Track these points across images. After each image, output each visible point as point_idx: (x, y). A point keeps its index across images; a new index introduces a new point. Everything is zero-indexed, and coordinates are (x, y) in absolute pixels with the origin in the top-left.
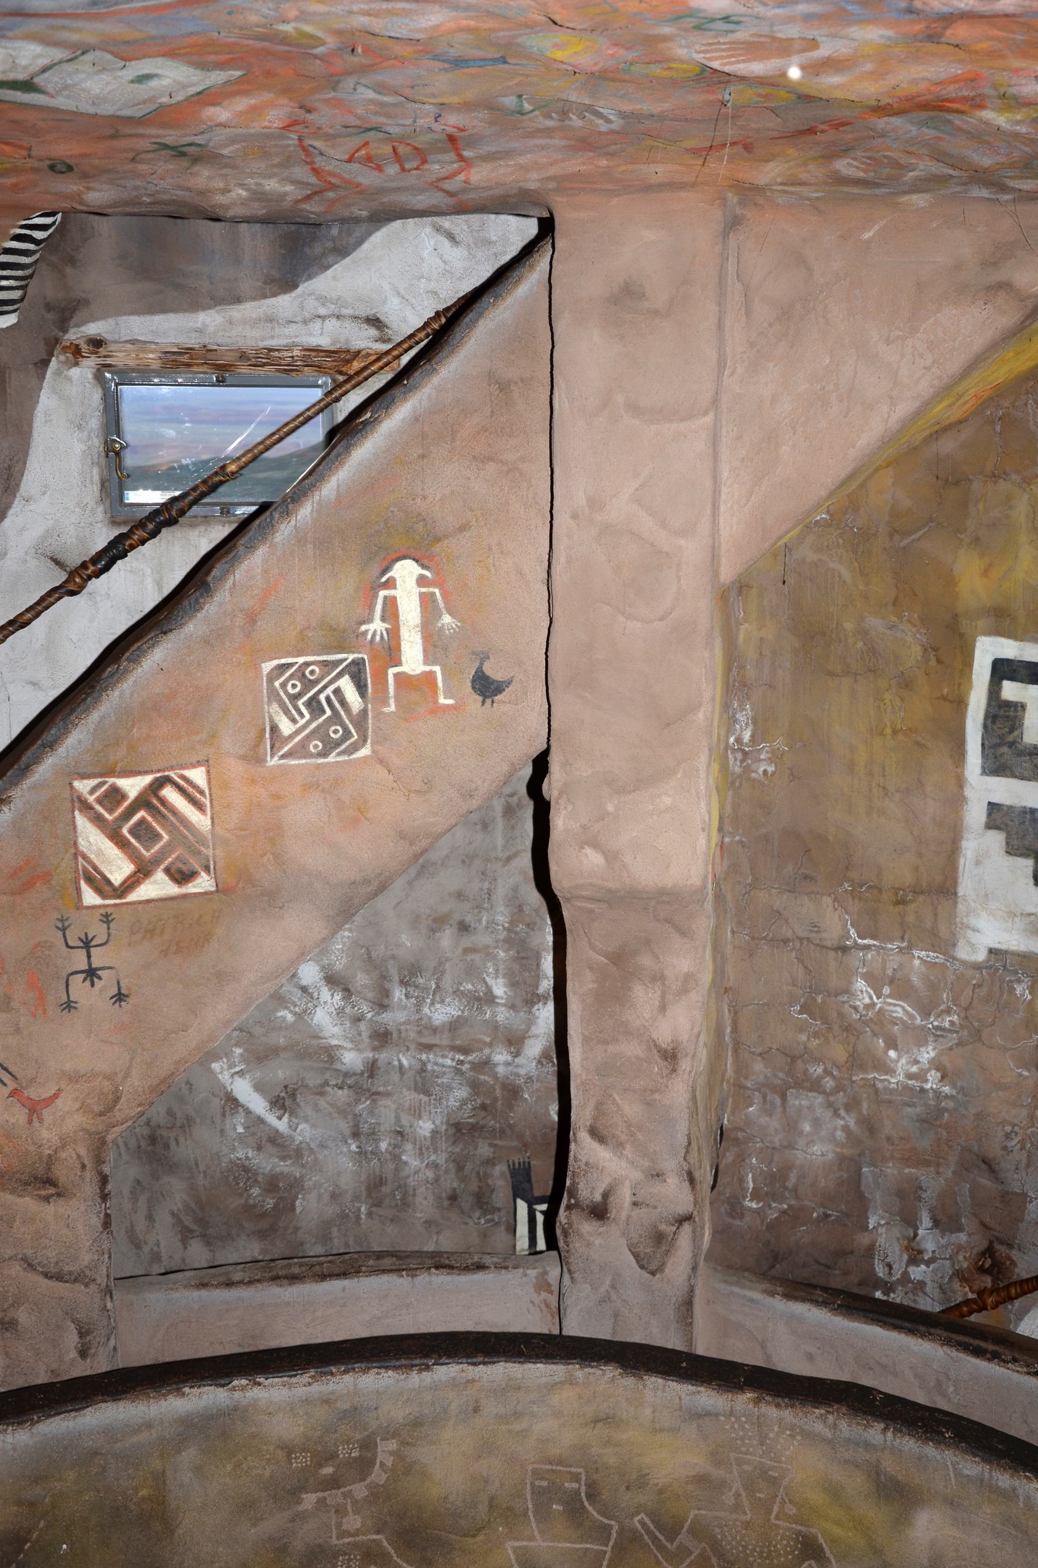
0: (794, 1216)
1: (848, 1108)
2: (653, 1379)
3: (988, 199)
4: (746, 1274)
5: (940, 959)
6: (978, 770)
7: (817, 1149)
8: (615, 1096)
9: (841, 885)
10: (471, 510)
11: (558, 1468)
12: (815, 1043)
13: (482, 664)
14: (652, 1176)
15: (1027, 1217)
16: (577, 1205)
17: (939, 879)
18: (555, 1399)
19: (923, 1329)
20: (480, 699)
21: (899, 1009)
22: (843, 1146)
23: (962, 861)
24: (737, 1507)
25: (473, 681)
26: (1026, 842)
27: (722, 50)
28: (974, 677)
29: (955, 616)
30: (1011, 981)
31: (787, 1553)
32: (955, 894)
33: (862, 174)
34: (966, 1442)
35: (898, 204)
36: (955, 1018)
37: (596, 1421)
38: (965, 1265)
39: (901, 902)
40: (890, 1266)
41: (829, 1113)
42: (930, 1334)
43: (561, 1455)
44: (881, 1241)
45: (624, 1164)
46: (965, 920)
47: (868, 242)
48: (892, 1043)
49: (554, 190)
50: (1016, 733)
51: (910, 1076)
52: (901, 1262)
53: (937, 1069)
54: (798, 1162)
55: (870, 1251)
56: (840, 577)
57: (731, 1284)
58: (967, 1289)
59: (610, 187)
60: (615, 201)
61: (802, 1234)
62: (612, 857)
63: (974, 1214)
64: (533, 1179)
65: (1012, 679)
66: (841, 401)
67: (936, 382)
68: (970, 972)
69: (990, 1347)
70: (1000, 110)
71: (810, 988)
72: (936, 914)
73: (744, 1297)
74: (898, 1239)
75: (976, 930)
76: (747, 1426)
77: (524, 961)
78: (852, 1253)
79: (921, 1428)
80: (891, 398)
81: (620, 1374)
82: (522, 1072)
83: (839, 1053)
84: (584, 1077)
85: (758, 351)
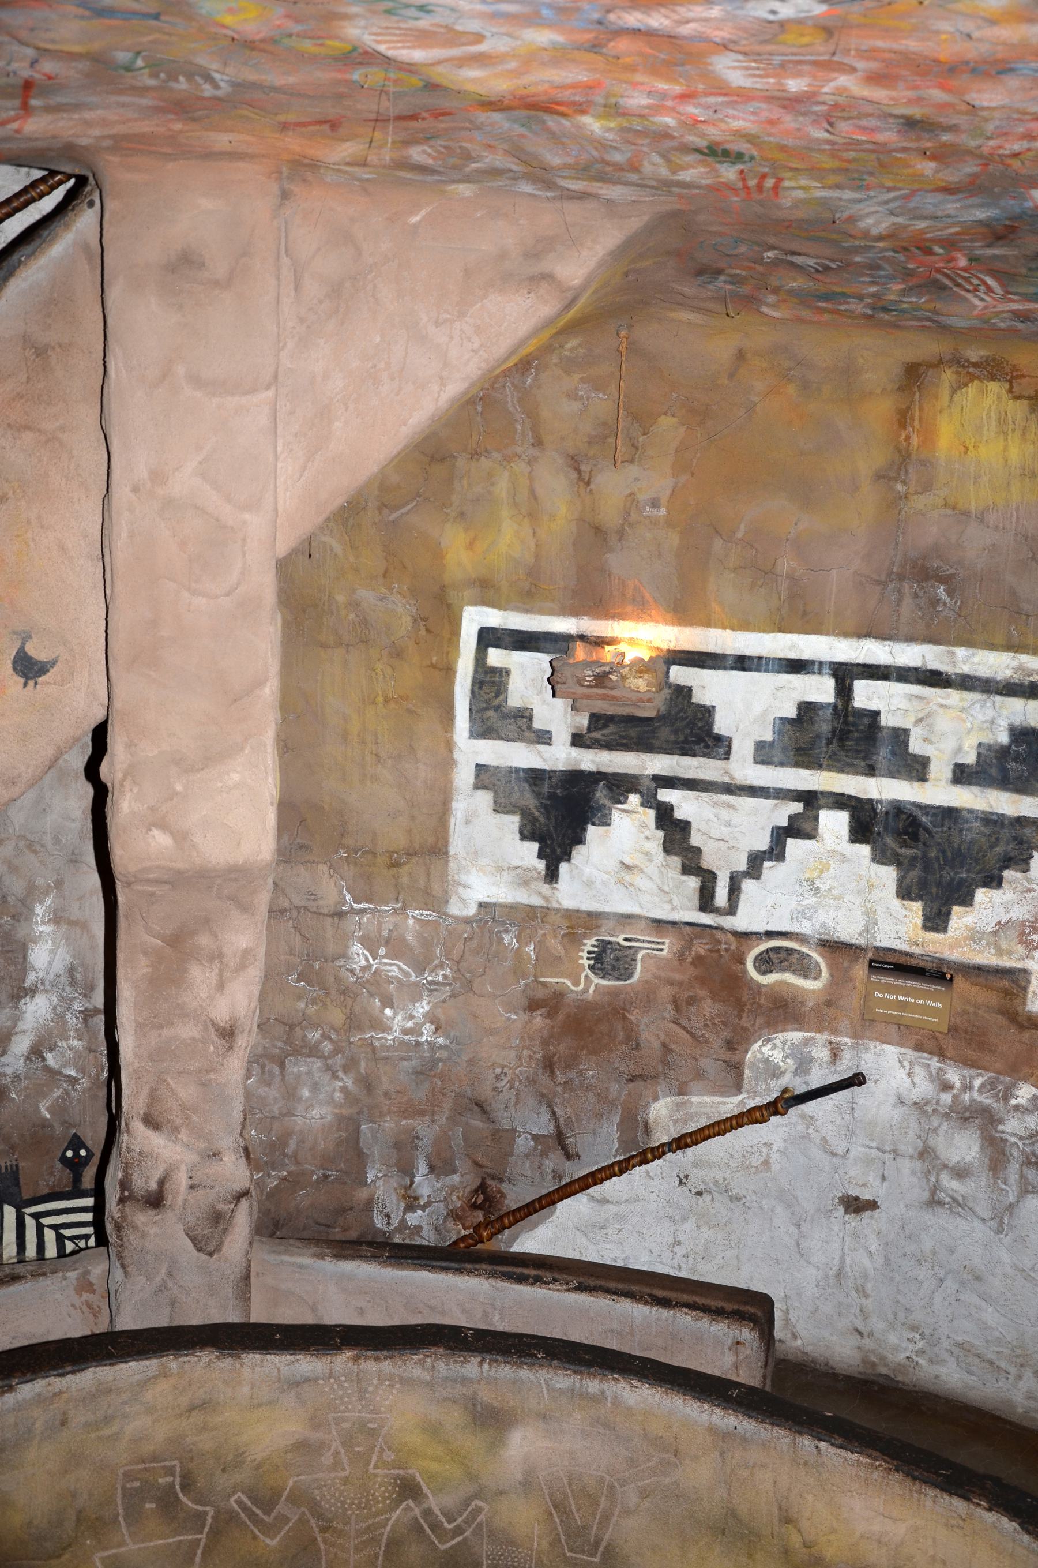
0: (292, 1183)
1: (346, 1069)
2: (251, 1356)
3: (530, 195)
4: (291, 1241)
5: (433, 916)
6: (466, 734)
7: (315, 1113)
8: (169, 1080)
9: (337, 852)
10: (7, 481)
11: (152, 1465)
12: (313, 1009)
13: (23, 644)
14: (209, 1156)
16: (131, 1197)
17: (431, 840)
18: (148, 1396)
19: (469, 1266)
20: (22, 680)
22: (341, 1106)
23: (452, 821)
24: (336, 1465)
25: (15, 662)
26: (513, 800)
27: (395, 35)
28: (461, 645)
29: (443, 588)
30: (500, 932)
31: (385, 1498)
32: (447, 853)
33: (431, 161)
34: (558, 1359)
35: (446, 191)
36: (448, 972)
37: (192, 1409)
38: (459, 1204)
39: (396, 865)
40: (388, 1216)
41: (327, 1077)
42: (476, 1270)
43: (154, 1452)
44: (379, 1193)
45: (179, 1148)
46: (456, 878)
47: (416, 226)
48: (388, 1002)
49: (108, 148)
50: (501, 697)
51: (405, 1032)
52: (398, 1209)
53: (432, 1023)
54: (297, 1128)
55: (369, 1205)
56: (332, 550)
57: (280, 1253)
58: (460, 1226)
59: (169, 150)
60: (170, 165)
61: (303, 1198)
62: (181, 837)
63: (467, 1155)
64: (22, 1181)
65: (497, 646)
66: (393, 379)
67: (483, 365)
68: (462, 927)
69: (533, 1272)
70: (598, 117)
71: (308, 955)
72: (428, 874)
73: (293, 1264)
74: (395, 1189)
75: (466, 886)
76: (346, 1385)
77: (10, 955)
78: (351, 1209)
79: (515, 1353)
80: (441, 378)
81: (217, 1357)
82: (9, 1071)
83: (337, 1016)
84: (136, 1064)
85: (308, 327)
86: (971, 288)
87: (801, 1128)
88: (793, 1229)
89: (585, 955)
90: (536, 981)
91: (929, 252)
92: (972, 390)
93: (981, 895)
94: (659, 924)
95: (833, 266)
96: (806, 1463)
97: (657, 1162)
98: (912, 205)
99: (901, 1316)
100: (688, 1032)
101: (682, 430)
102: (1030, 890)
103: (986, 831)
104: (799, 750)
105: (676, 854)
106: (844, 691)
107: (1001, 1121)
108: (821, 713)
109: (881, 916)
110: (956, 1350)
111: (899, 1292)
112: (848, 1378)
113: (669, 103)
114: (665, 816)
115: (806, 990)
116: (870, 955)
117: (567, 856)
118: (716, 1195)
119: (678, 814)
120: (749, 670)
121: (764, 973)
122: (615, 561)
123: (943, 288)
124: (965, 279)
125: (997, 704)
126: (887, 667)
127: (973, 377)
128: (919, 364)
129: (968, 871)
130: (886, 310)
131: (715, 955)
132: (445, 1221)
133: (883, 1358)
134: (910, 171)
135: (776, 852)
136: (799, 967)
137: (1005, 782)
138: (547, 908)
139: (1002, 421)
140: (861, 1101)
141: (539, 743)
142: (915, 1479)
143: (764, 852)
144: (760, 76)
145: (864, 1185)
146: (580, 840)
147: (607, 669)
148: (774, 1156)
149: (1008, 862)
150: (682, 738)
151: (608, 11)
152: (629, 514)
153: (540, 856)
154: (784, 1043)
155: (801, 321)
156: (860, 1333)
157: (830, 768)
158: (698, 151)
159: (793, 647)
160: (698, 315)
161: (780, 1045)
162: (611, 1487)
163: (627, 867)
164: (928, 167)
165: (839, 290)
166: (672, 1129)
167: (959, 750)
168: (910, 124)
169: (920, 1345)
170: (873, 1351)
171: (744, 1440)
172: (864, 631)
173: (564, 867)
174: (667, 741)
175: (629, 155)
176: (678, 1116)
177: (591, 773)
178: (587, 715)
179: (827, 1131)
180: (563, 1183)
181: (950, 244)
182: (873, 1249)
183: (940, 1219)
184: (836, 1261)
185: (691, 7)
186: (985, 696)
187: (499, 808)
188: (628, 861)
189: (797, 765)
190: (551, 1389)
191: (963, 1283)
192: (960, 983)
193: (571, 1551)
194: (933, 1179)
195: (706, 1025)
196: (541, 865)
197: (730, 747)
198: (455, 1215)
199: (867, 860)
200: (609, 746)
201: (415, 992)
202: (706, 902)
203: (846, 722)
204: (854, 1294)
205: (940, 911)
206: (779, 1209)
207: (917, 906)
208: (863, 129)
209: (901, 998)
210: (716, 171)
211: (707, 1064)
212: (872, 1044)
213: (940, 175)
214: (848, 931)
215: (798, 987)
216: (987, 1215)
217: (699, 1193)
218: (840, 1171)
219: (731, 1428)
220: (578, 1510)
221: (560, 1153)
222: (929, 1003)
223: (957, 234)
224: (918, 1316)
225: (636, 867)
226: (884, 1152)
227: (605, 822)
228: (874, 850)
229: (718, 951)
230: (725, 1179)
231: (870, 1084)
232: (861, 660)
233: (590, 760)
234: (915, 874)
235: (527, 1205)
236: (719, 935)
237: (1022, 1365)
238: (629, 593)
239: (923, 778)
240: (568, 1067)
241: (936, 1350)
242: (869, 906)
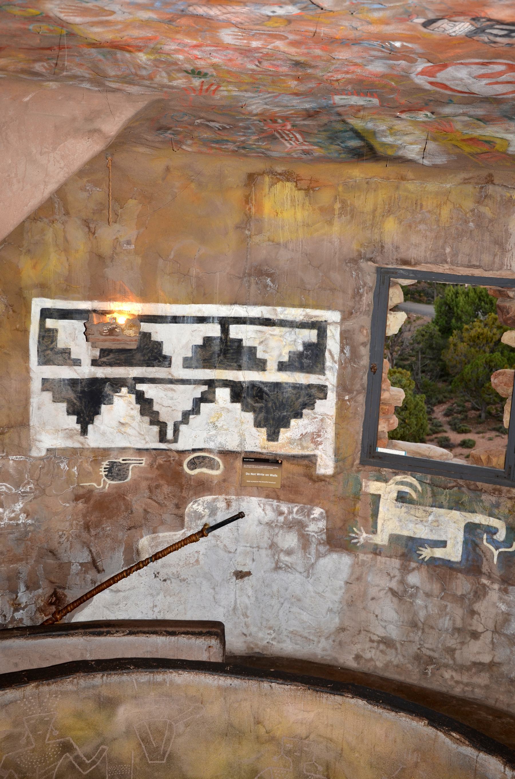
5: (23, 458)
6: (36, 363)
15: (71, 573)
17: (20, 419)
19: (72, 632)
21: (3, 487)
23: (31, 408)
24: (28, 743)
26: (62, 395)
27: (71, 9)
29: (21, 289)
30: (58, 463)
31: (54, 755)
32: (29, 425)
38: (42, 604)
40: (5, 616)
46: (34, 437)
47: (27, 103)
50: (54, 344)
51: (11, 519)
52: (10, 611)
53: (24, 513)
66: (19, 182)
67: (66, 175)
69: (105, 630)
70: (146, 53)
72: (20, 437)
75: (39, 441)
80: (45, 182)
86: (288, 139)
87: (213, 542)
88: (211, 591)
89: (103, 470)
90: (78, 485)
91: (275, 122)
92: (279, 186)
93: (293, 422)
94: (140, 451)
95: (228, 127)
96: (266, 695)
97: (145, 567)
98: (276, 100)
99: (264, 623)
100: (156, 502)
101: (140, 206)
102: (315, 418)
103: (295, 392)
104: (205, 360)
105: (146, 415)
106: (225, 330)
107: (307, 526)
108: (214, 342)
109: (247, 437)
110: (290, 635)
111: (263, 612)
112: (241, 657)
113: (186, 49)
114: (140, 397)
115: (212, 476)
116: (243, 455)
117: (91, 421)
118: (173, 580)
119: (147, 396)
120: (179, 323)
121: (192, 469)
122: (110, 272)
123: (276, 138)
124: (287, 135)
125: (297, 333)
126: (245, 318)
127: (279, 180)
128: (254, 174)
129: (287, 411)
130: (244, 148)
131: (168, 463)
132: (35, 614)
133: (256, 645)
134: (285, 85)
135: (196, 410)
136: (209, 465)
137: (303, 369)
138: (83, 448)
139: (293, 201)
140: (242, 525)
141: (74, 365)
142: (317, 691)
143: (190, 411)
144: (241, 39)
145: (244, 565)
146: (98, 413)
147: (114, 326)
148: (201, 557)
149: (305, 406)
150: (147, 358)
151: (189, 6)
152: (116, 248)
153: (77, 423)
154: (203, 502)
155: (201, 153)
156: (245, 635)
157: (220, 368)
158: (186, 72)
159: (200, 310)
160: (148, 150)
161: (201, 503)
162: (171, 725)
163: (122, 424)
164: (293, 84)
165: (225, 138)
166: (150, 551)
167: (280, 355)
168: (297, 64)
169: (273, 636)
170: (252, 642)
171: (235, 689)
172: (233, 302)
173: (90, 427)
174: (140, 360)
175: (151, 72)
176: (153, 544)
177: (102, 379)
178: (99, 350)
179: (227, 542)
180: (96, 585)
181: (286, 118)
182: (250, 594)
183: (282, 575)
184: (233, 603)
185: (235, 7)
186: (291, 329)
187: (55, 400)
188: (122, 421)
189: (204, 367)
190: (138, 683)
191: (292, 604)
192: (285, 464)
193: (151, 760)
194: (276, 557)
195: (165, 498)
196: (78, 427)
197: (171, 361)
198: (41, 610)
199: (240, 410)
200: (111, 365)
201: (15, 498)
202: (162, 438)
203: (226, 346)
204: (242, 617)
205: (275, 432)
206: (204, 582)
207: (264, 430)
208: (274, 65)
209: (258, 474)
210: (191, 81)
211: (167, 517)
212: (245, 498)
213: (297, 88)
214: (232, 445)
215: (209, 474)
216: (302, 570)
217: (165, 580)
218: (233, 560)
219: (229, 685)
220: (154, 740)
221: (94, 571)
222: (271, 475)
223: (292, 114)
224: (272, 623)
225: (127, 423)
226: (253, 548)
227: (110, 402)
228: (242, 405)
229: (170, 461)
230: (177, 572)
231: (246, 516)
232: (232, 315)
233: (101, 372)
234: (262, 415)
235: (80, 599)
236: (169, 453)
237: (320, 636)
238: (118, 288)
239: (264, 370)
240: (97, 527)
241: (281, 636)
242: (241, 432)
